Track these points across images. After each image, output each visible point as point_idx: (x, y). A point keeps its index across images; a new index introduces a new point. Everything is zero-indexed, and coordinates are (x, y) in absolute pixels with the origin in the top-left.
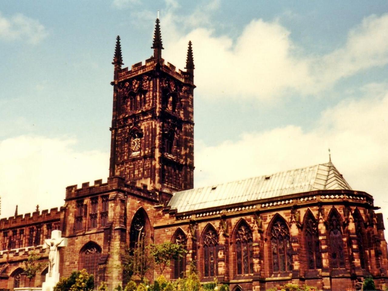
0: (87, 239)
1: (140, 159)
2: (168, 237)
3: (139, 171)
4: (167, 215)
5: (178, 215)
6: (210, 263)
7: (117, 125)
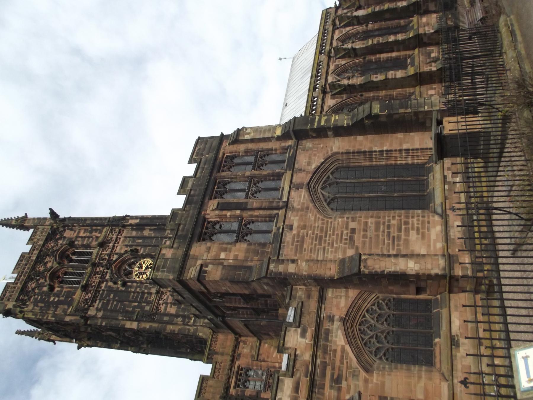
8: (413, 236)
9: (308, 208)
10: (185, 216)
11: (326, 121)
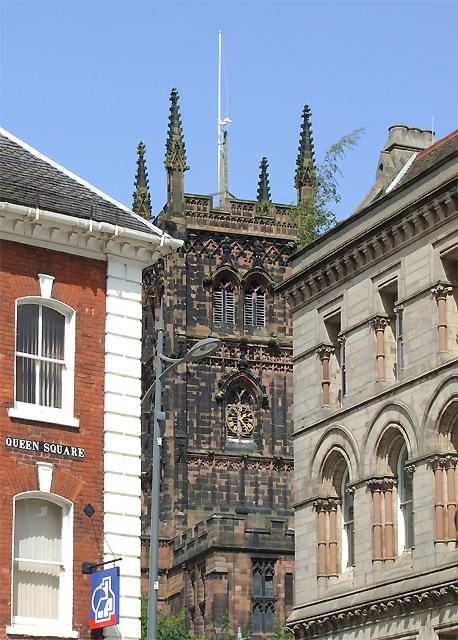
1: (264, 462)
3: (256, 491)
10: (279, 537)
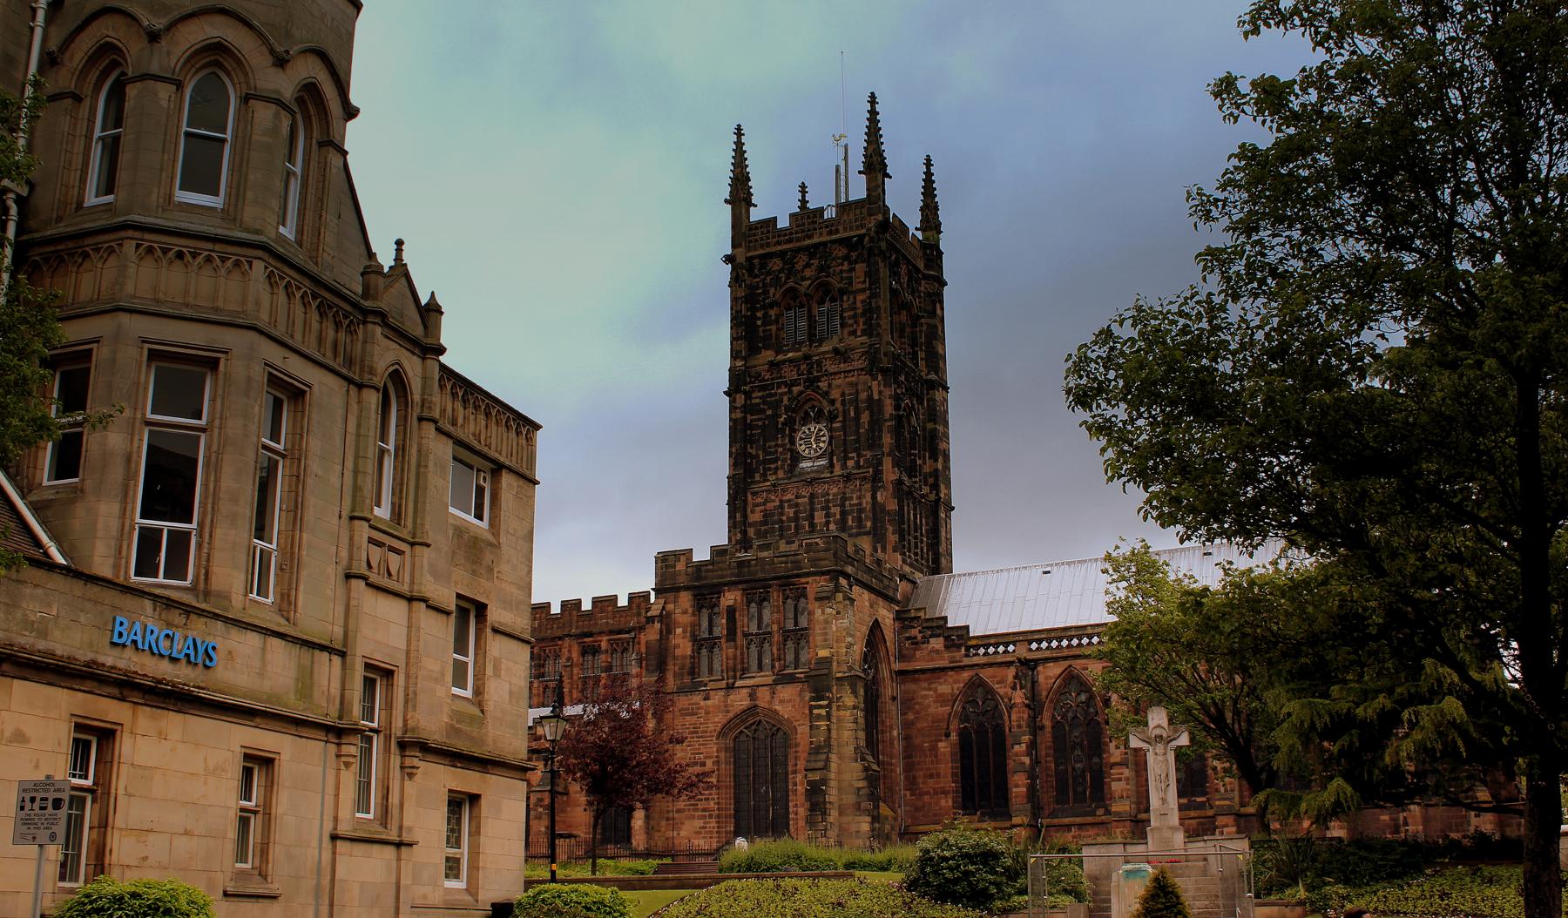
0: (740, 701)
2: (941, 699)
3: (827, 516)
4: (937, 643)
5: (973, 642)
6: (1073, 769)
7: (748, 380)
8: (698, 823)
9: (728, 712)
11: (819, 715)
